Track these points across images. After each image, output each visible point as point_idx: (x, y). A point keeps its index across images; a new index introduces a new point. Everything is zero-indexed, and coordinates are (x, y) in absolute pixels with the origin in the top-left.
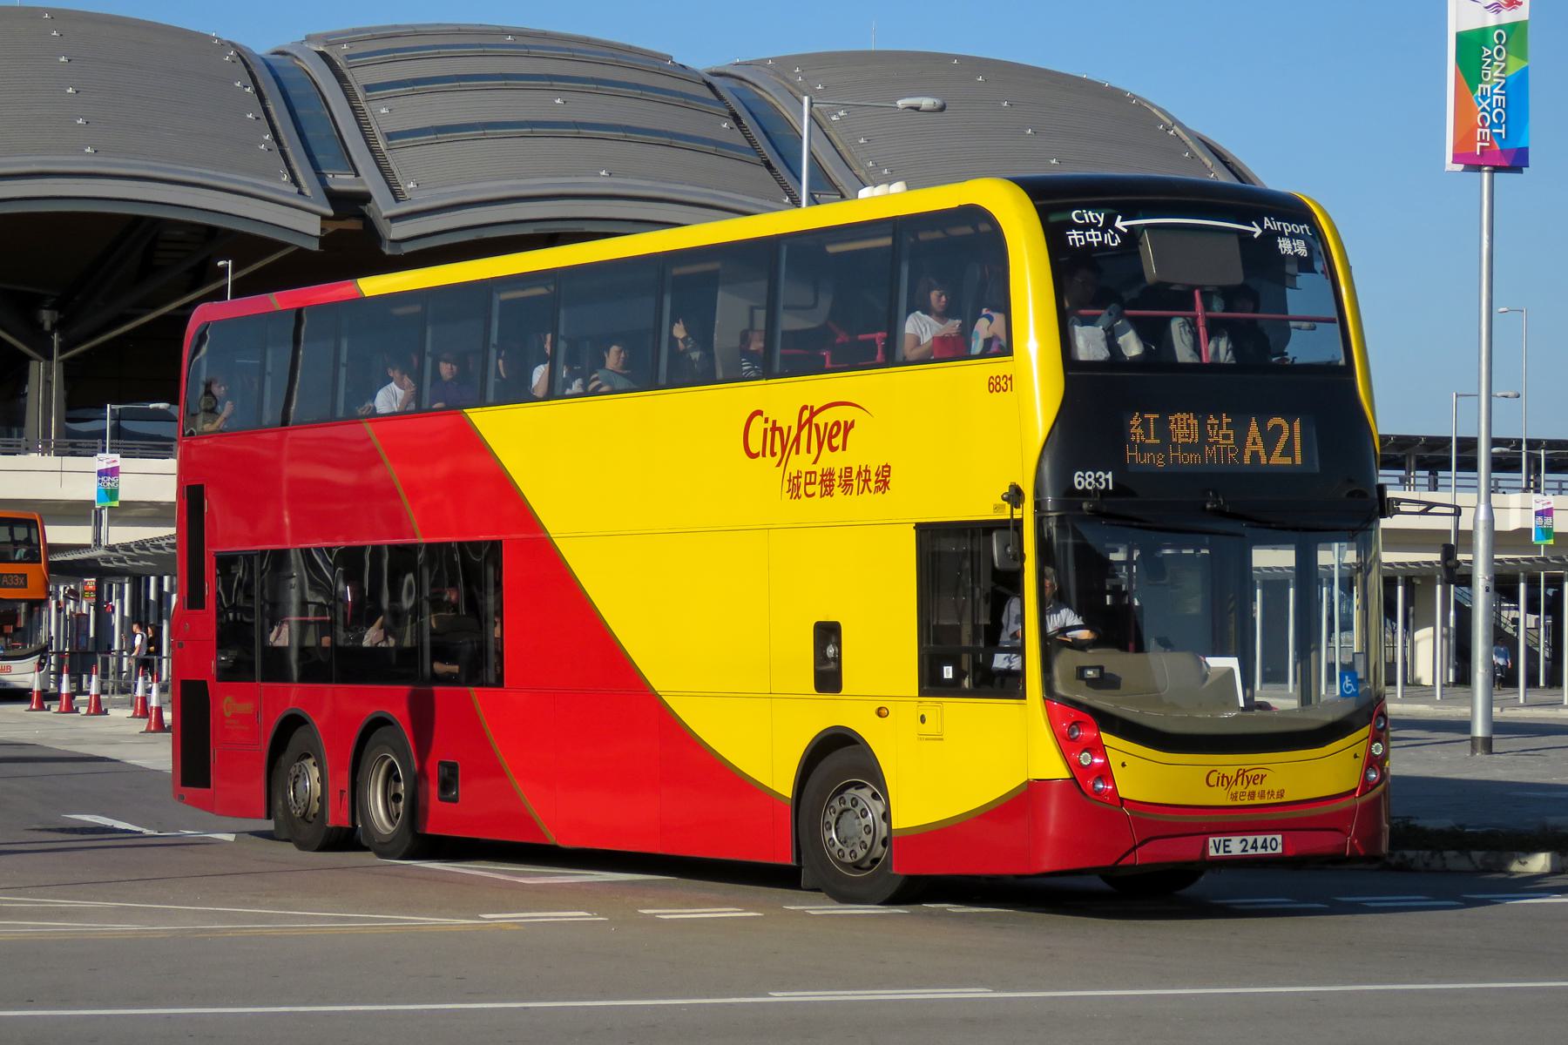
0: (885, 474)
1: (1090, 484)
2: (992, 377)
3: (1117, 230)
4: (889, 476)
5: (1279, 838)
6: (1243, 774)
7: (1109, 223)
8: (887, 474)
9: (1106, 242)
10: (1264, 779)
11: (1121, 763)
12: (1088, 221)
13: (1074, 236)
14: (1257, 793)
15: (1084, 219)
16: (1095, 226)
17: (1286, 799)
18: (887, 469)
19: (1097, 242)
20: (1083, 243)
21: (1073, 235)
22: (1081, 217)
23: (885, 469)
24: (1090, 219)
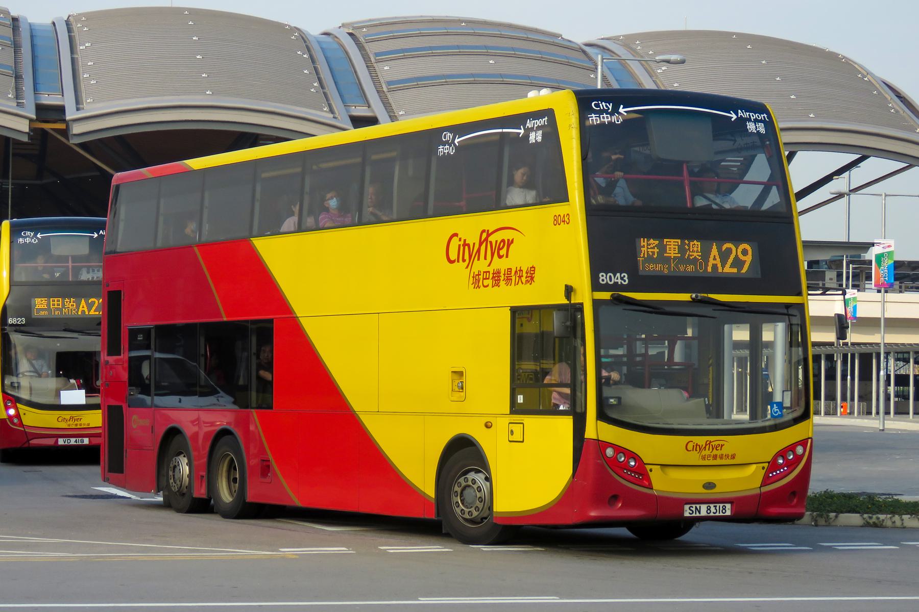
0: (532, 272)
4: (534, 273)
8: (533, 272)
18: (533, 269)
23: (533, 269)
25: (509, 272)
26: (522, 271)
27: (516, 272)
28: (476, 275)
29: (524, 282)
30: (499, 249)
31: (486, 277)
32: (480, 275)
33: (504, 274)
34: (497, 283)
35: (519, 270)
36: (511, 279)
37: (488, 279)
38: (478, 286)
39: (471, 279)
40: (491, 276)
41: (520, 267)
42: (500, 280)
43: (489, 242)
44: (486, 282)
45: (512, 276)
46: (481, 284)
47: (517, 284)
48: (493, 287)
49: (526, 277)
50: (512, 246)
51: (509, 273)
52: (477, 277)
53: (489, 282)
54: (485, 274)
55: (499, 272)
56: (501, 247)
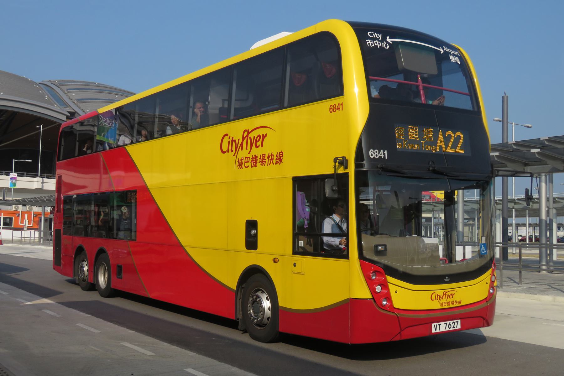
0: (281, 156)
1: (377, 155)
2: (332, 106)
3: (387, 42)
4: (282, 156)
5: (459, 321)
6: (445, 294)
7: (384, 39)
8: (281, 156)
9: (383, 47)
10: (454, 295)
11: (395, 292)
12: (375, 37)
13: (369, 42)
14: (451, 302)
15: (373, 36)
16: (378, 39)
17: (462, 304)
18: (282, 153)
19: (379, 46)
20: (373, 46)
21: (369, 42)
22: (371, 34)
23: (282, 153)
24: (376, 36)
25: (264, 156)
26: (273, 155)
27: (269, 156)
28: (240, 160)
29: (275, 164)
30: (256, 142)
31: (247, 160)
32: (243, 160)
33: (260, 158)
34: (254, 164)
35: (271, 155)
36: (265, 161)
37: (249, 162)
38: (241, 167)
39: (237, 163)
40: (251, 160)
41: (272, 153)
42: (257, 162)
43: (249, 138)
44: (247, 164)
45: (265, 160)
46: (243, 165)
47: (270, 165)
48: (252, 167)
49: (276, 160)
50: (266, 138)
51: (263, 157)
52: (241, 161)
53: (249, 164)
54: (246, 159)
55: (256, 157)
56: (257, 140)
